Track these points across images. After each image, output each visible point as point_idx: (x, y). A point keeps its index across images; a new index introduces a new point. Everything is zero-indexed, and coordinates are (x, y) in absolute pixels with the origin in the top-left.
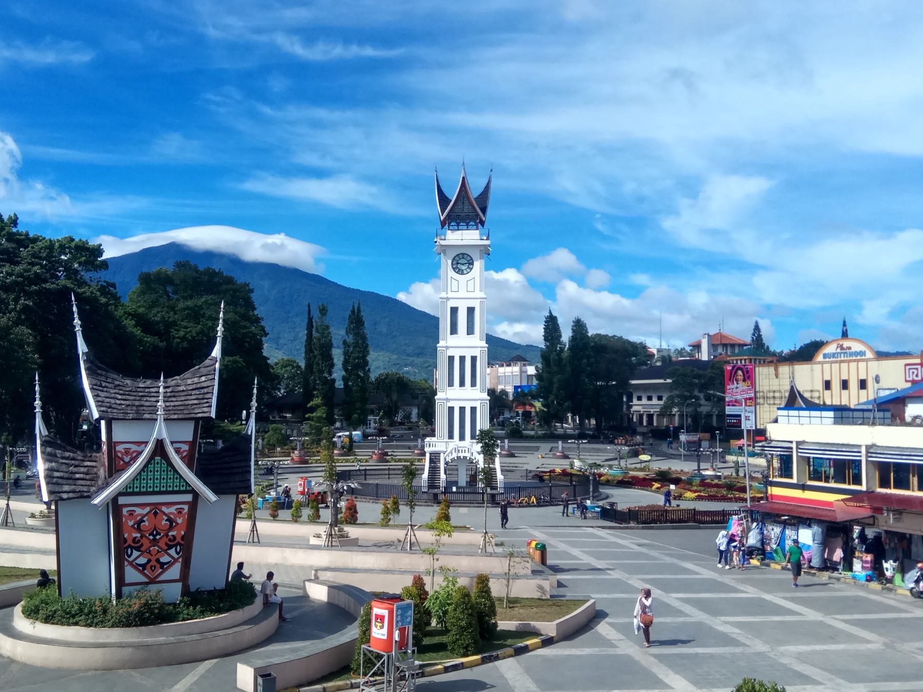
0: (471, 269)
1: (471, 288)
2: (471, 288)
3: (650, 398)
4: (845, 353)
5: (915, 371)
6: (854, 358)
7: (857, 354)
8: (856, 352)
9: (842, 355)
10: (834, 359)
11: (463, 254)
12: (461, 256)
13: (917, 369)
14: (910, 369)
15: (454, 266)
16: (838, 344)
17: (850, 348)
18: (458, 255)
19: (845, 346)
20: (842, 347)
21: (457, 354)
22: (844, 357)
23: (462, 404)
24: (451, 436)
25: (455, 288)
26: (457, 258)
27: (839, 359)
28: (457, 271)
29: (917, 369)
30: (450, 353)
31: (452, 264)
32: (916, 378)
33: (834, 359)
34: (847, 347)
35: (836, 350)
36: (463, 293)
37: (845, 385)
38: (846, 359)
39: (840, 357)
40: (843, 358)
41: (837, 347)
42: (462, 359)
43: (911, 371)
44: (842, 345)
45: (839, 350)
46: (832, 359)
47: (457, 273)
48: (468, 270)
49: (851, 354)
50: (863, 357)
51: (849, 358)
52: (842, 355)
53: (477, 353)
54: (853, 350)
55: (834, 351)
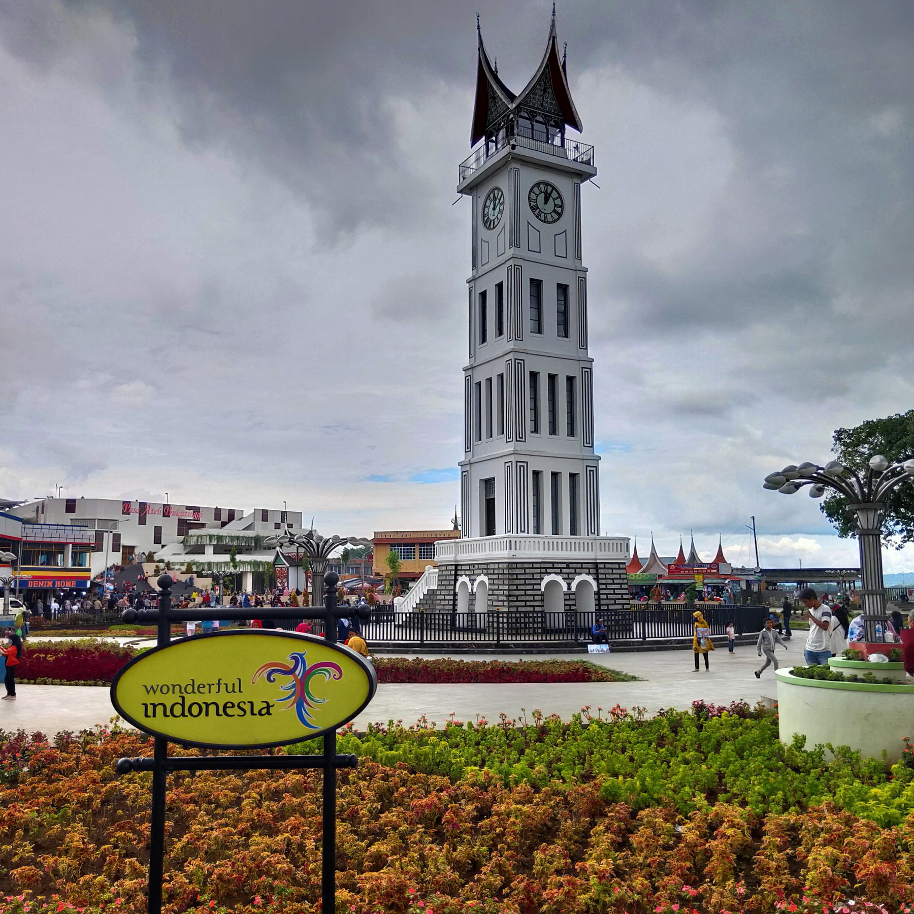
0: (560, 215)
1: (561, 252)
2: (561, 252)
11: (547, 184)
12: (542, 186)
15: (532, 204)
18: (537, 185)
21: (544, 369)
24: (538, 530)
25: (534, 246)
26: (536, 190)
28: (536, 213)
30: (530, 367)
31: (530, 200)
36: (547, 256)
42: (552, 378)
47: (537, 217)
48: (556, 217)
53: (576, 372)
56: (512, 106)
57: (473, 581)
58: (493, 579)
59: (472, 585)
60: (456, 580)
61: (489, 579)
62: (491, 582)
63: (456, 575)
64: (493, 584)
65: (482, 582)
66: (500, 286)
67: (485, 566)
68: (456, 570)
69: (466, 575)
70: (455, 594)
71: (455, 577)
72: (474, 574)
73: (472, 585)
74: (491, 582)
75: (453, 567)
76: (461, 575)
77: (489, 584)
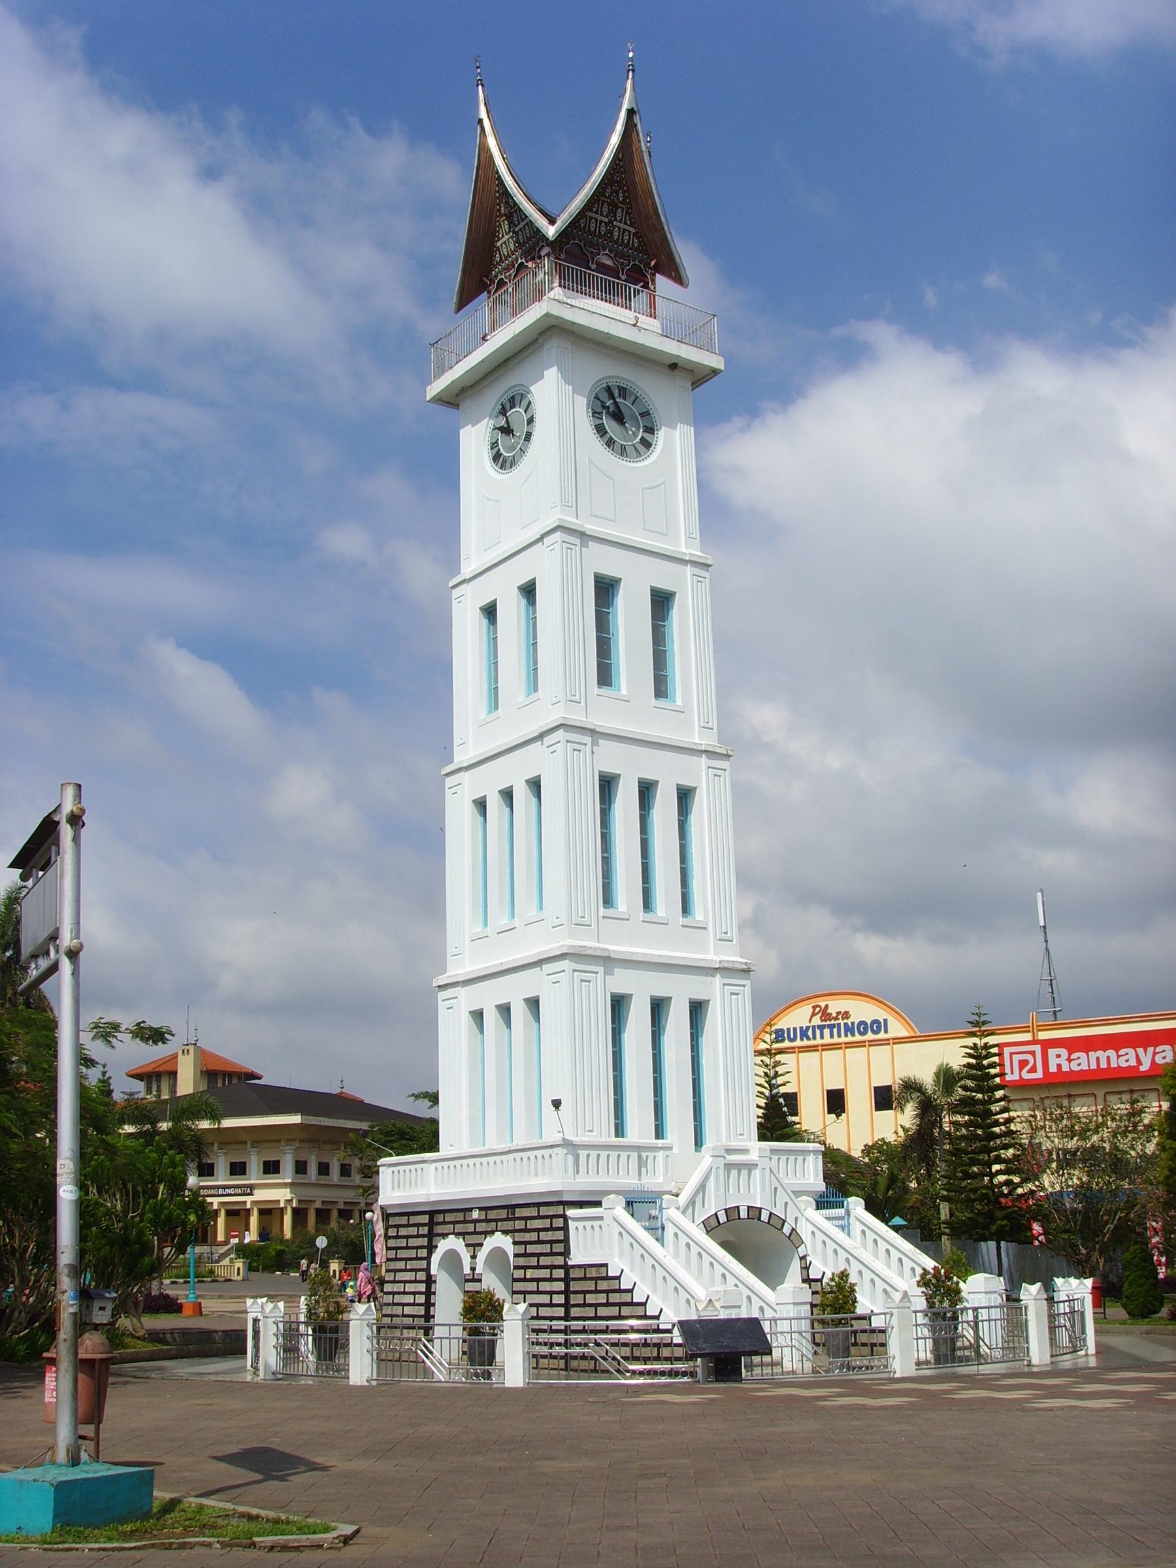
3: (238, 1169)
4: (831, 1027)
5: (1029, 1057)
6: (858, 1038)
7: (863, 1027)
8: (862, 1023)
9: (827, 1031)
10: (806, 1043)
13: (1033, 1053)
14: (1011, 1054)
16: (814, 1007)
17: (846, 1015)
19: (832, 1010)
20: (825, 1015)
22: (832, 1036)
23: (661, 984)
27: (818, 1041)
29: (1033, 1053)
32: (1026, 1076)
33: (806, 1043)
34: (838, 1013)
35: (810, 1021)
37: (836, 1102)
38: (836, 1040)
39: (822, 1037)
40: (827, 1040)
41: (813, 1014)
43: (1016, 1058)
44: (827, 1006)
45: (817, 1021)
46: (798, 1043)
49: (849, 1030)
50: (882, 1035)
51: (843, 1039)
52: (827, 1031)
54: (855, 1018)
55: (805, 1024)
56: (551, 232)
57: (475, 1247)
58: (526, 1243)
59: (474, 1257)
60: (431, 1248)
61: (515, 1243)
62: (521, 1249)
63: (431, 1235)
64: (525, 1255)
65: (498, 1252)
66: (529, 591)
67: (503, 1214)
68: (431, 1224)
69: (457, 1234)
70: (430, 1281)
71: (430, 1241)
72: (475, 1233)
73: (474, 1257)
74: (521, 1249)
75: (425, 1219)
76: (444, 1236)
77: (516, 1255)
